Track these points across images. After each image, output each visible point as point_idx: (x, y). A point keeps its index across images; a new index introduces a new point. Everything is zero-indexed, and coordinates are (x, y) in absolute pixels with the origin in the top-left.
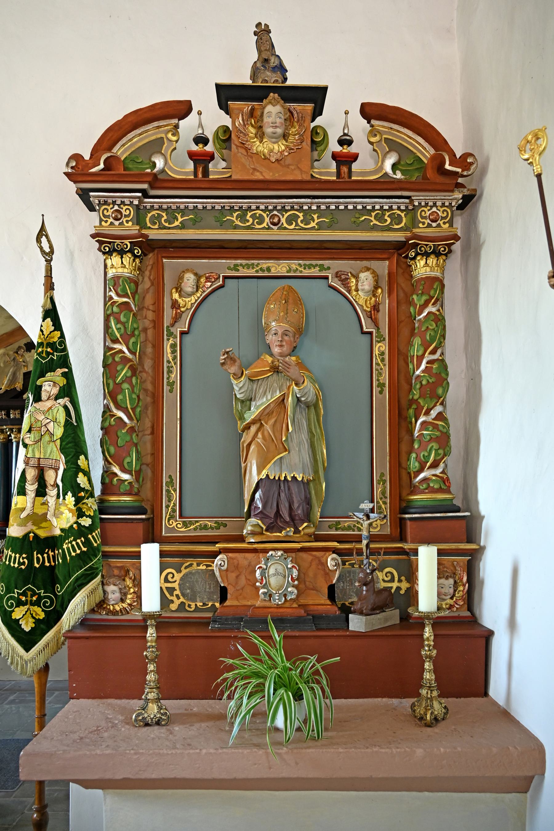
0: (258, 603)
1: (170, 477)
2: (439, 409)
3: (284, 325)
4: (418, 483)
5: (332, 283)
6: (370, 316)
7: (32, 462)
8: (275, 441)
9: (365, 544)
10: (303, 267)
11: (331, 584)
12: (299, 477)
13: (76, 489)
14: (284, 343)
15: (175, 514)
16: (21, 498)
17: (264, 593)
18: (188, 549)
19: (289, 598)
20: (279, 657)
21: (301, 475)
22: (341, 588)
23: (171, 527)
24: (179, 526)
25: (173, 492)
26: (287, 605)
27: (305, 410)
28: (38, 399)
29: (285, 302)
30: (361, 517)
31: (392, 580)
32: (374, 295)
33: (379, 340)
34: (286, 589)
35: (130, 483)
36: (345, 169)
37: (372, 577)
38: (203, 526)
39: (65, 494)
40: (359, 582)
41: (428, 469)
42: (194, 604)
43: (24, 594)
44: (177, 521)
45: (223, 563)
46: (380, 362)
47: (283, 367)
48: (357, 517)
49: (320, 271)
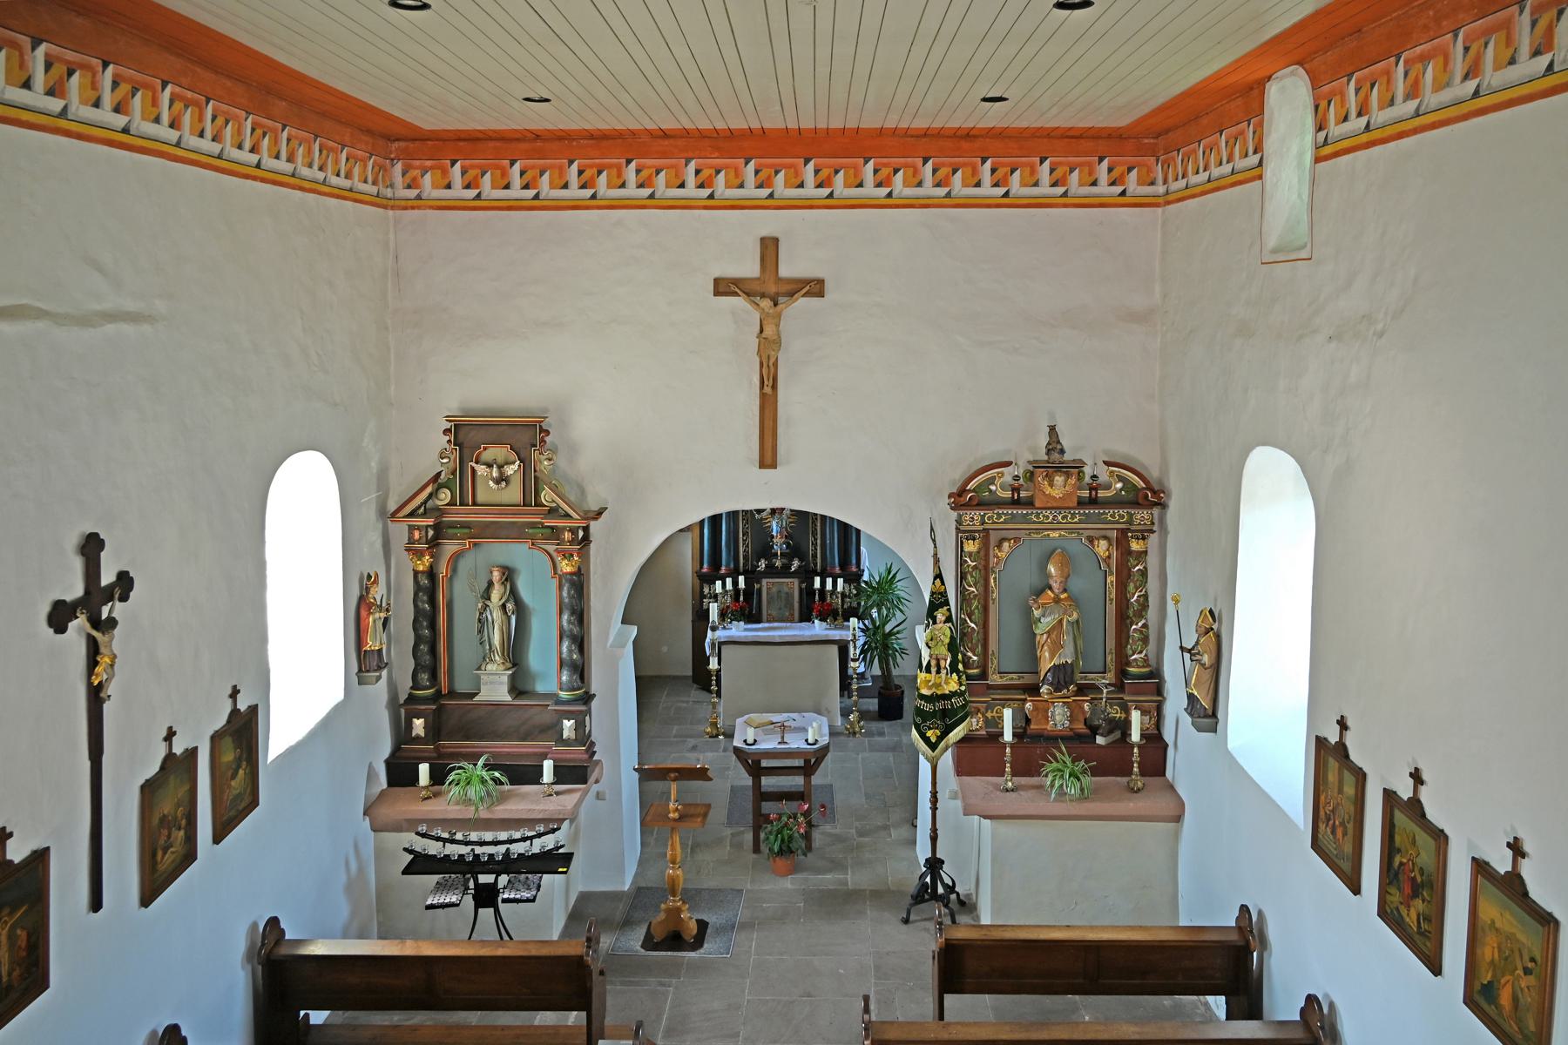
2: (1143, 621)
6: (1105, 561)
7: (934, 657)
13: (958, 672)
16: (928, 675)
20: (1068, 760)
28: (935, 623)
31: (1117, 713)
36: (1094, 493)
39: (951, 674)
43: (932, 724)
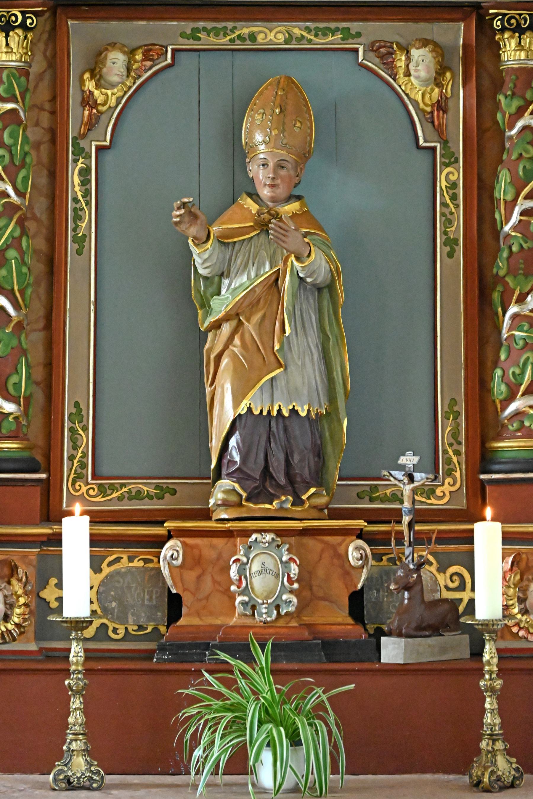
0: (234, 621)
1: (77, 404)
3: (279, 151)
4: (508, 420)
5: (364, 61)
8: (263, 351)
9: (406, 523)
10: (313, 32)
11: (353, 590)
12: (303, 410)
14: (279, 181)
15: (84, 471)
17: (244, 604)
18: (115, 532)
19: (283, 612)
21: (306, 407)
22: (373, 600)
23: (77, 494)
24: (91, 492)
25: (81, 432)
26: (281, 623)
27: (313, 294)
29: (281, 111)
30: (401, 478)
32: (439, 84)
33: (447, 161)
34: (280, 596)
35: (16, 418)
37: (419, 576)
38: (133, 494)
40: (396, 583)
41: (523, 395)
42: (123, 627)
44: (87, 484)
45: (176, 554)
46: (448, 201)
47: (276, 234)
48: (395, 478)
49: (343, 39)
